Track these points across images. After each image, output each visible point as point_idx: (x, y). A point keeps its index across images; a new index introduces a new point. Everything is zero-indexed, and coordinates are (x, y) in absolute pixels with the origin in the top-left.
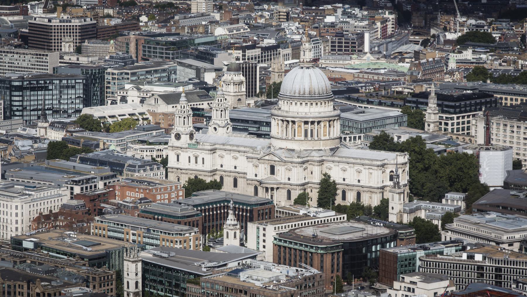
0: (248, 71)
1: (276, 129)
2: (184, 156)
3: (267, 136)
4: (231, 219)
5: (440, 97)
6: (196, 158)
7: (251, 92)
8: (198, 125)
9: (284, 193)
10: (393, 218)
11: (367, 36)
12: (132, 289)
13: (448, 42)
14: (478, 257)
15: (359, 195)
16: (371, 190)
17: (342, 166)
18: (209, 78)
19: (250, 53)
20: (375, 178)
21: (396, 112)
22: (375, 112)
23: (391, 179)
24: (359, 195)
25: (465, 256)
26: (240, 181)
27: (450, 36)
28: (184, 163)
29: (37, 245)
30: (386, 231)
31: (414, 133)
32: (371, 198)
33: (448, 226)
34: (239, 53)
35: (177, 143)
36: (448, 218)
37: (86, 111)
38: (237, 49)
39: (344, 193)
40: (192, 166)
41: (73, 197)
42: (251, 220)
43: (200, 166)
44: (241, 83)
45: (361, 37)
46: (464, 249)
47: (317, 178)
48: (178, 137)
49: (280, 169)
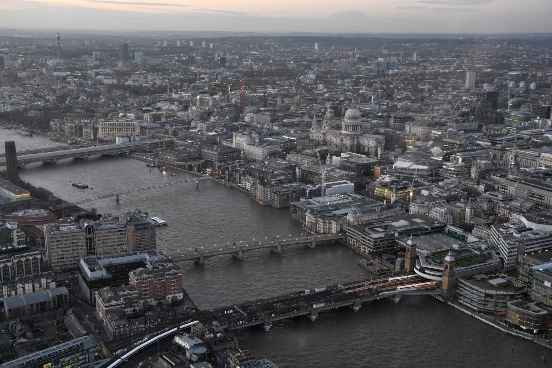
1: (343, 127)
4: (329, 156)
5: (395, 117)
7: (335, 115)
9: (345, 147)
11: (373, 97)
12: (298, 177)
13: (398, 99)
15: (369, 149)
19: (336, 102)
24: (369, 149)
27: (399, 97)
30: (377, 160)
35: (313, 132)
40: (317, 138)
41: (280, 148)
43: (319, 139)
47: (355, 143)
48: (313, 129)
49: (344, 140)
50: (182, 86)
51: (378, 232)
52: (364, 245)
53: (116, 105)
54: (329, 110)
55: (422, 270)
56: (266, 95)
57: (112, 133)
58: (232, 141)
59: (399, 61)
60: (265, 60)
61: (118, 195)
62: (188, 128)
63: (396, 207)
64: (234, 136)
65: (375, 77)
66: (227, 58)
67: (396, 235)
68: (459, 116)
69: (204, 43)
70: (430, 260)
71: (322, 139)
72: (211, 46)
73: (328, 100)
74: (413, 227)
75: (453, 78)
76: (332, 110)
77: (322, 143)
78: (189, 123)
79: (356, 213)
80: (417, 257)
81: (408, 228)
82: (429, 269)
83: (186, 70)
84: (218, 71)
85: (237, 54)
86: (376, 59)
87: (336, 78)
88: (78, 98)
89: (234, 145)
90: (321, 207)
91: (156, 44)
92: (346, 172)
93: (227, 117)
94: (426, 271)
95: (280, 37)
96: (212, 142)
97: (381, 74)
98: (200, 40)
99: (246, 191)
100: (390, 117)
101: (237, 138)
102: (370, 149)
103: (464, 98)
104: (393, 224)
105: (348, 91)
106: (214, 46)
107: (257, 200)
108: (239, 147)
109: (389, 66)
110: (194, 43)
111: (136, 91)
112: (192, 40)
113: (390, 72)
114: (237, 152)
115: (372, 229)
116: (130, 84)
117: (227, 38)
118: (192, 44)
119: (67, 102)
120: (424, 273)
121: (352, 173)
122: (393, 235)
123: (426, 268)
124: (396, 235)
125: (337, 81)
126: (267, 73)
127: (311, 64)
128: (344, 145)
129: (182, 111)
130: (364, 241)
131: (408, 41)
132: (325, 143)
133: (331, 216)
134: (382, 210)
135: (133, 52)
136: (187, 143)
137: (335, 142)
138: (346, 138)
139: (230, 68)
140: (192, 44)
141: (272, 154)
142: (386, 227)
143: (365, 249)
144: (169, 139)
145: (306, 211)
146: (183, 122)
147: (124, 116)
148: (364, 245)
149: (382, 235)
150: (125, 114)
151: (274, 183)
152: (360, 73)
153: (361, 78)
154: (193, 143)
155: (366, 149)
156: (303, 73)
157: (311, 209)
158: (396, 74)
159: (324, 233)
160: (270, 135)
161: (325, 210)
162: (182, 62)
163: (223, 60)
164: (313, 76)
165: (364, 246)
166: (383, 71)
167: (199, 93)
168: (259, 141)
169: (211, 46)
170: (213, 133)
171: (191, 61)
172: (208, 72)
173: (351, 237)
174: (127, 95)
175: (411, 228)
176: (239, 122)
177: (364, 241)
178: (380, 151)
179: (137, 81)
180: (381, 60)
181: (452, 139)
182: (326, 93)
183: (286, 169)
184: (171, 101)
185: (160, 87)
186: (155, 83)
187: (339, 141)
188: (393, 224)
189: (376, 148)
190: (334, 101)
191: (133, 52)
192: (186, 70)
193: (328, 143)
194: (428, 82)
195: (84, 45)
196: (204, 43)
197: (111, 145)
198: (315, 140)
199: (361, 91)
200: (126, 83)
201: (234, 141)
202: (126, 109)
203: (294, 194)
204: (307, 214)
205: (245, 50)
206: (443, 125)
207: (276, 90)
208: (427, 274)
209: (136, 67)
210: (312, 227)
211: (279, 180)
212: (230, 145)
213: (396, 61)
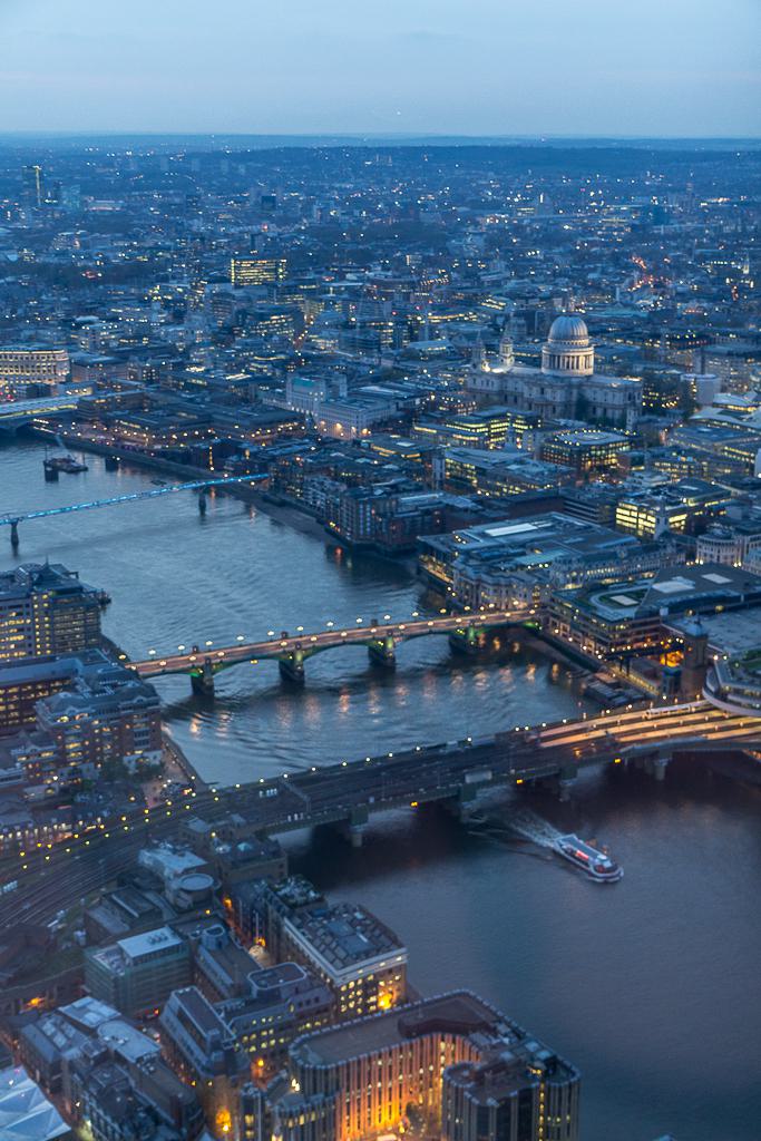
0: (528, 316)
1: (544, 360)
2: (479, 381)
6: (488, 381)
9: (550, 408)
15: (605, 410)
16: (614, 407)
17: (594, 389)
18: (500, 321)
20: (619, 399)
23: (630, 398)
24: (605, 410)
26: (520, 400)
32: (613, 414)
34: (524, 301)
38: (522, 298)
39: (594, 409)
40: (484, 388)
41: (398, 409)
43: (490, 388)
44: (523, 325)
49: (548, 391)
51: (621, 606)
54: (513, 321)
58: (282, 397)
61: (14, 524)
62: (181, 366)
63: (665, 547)
64: (289, 385)
65: (628, 241)
67: (664, 612)
71: (496, 388)
72: (242, 170)
73: (512, 296)
74: (704, 594)
76: (522, 321)
78: (186, 354)
79: (570, 562)
80: (711, 663)
81: (691, 597)
82: (737, 692)
83: (179, 228)
84: (255, 228)
85: (299, 188)
90: (489, 548)
92: (552, 466)
94: (730, 697)
95: (404, 149)
97: (639, 232)
98: (218, 156)
99: (315, 511)
101: (297, 388)
102: (609, 414)
105: (560, 275)
109: (661, 216)
111: (63, 277)
113: (662, 230)
114: (295, 419)
115: (607, 600)
116: (47, 260)
122: (657, 613)
124: (664, 612)
126: (373, 235)
127: (477, 212)
128: (548, 403)
129: (167, 324)
134: (632, 554)
137: (526, 395)
138: (551, 386)
139: (281, 222)
140: (195, 165)
141: (379, 424)
142: (638, 595)
146: (171, 351)
149: (631, 613)
150: (32, 332)
151: (379, 492)
153: (592, 244)
154: (191, 400)
155: (599, 412)
156: (456, 232)
157: (467, 554)
158: (674, 237)
159: (496, 609)
160: (375, 380)
161: (500, 556)
164: (480, 242)
166: (644, 227)
168: (349, 395)
169: (242, 170)
170: (240, 376)
172: (233, 230)
175: (698, 595)
178: (631, 417)
179: (63, 253)
182: (509, 279)
184: (145, 303)
187: (535, 392)
188: (656, 586)
190: (527, 299)
191: (57, 186)
192: (179, 228)
193: (511, 399)
194: (750, 252)
198: (481, 392)
199: (591, 276)
203: (427, 518)
208: (732, 702)
209: (64, 223)
211: (392, 486)
212: (281, 405)
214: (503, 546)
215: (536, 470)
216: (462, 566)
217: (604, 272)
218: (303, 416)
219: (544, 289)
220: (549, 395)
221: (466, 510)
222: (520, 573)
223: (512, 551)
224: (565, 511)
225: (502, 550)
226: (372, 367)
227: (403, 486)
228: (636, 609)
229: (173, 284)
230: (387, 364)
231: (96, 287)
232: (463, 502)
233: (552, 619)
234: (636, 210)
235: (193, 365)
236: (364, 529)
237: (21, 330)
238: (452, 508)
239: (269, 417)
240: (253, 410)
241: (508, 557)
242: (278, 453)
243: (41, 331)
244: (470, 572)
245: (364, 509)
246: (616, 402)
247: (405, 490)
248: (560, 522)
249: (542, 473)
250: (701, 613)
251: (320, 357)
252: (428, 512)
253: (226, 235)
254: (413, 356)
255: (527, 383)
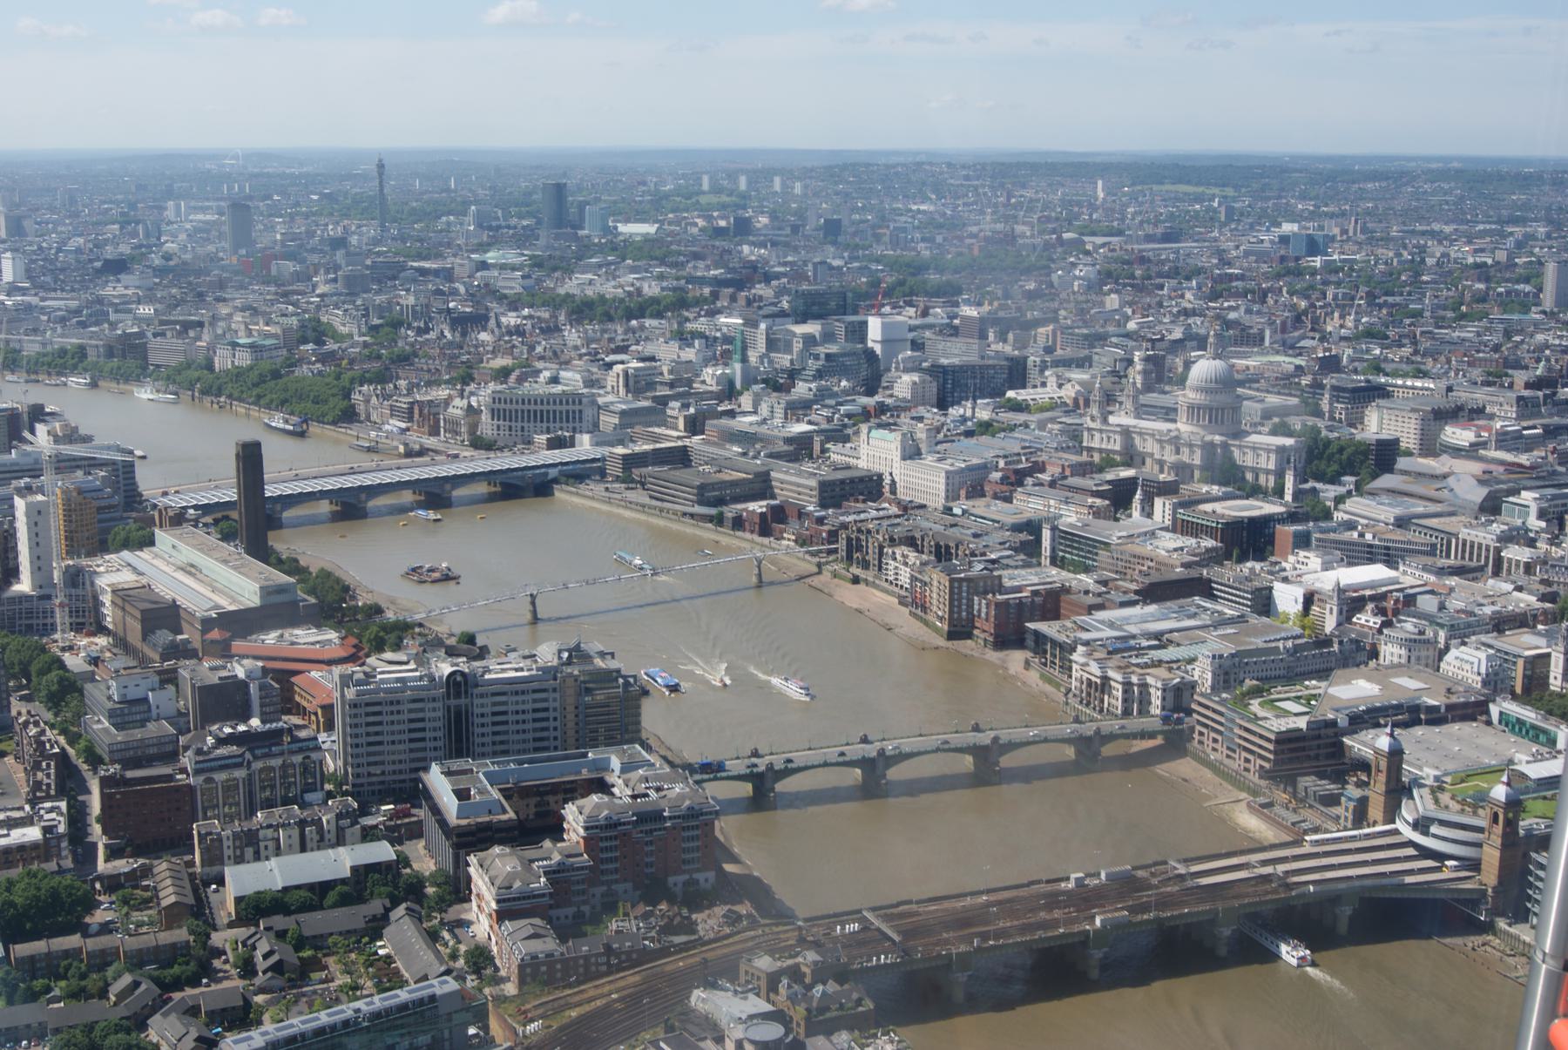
2: (1097, 435)
3: (1175, 421)
8: (1110, 409)
10: (1288, 497)
11: (1267, 333)
14: (1369, 536)
16: (1268, 472)
21: (1295, 401)
22: (1273, 400)
25: (1355, 535)
28: (1096, 444)
29: (964, 512)
30: (1282, 509)
31: (1311, 420)
33: (1341, 506)
35: (1092, 425)
36: (1339, 500)
37: (1010, 394)
42: (1159, 495)
45: (1262, 332)
46: (1355, 528)
48: (1093, 419)
50: (715, 296)
51: (1286, 713)
52: (1246, 749)
53: (532, 348)
55: (1421, 825)
56: (956, 322)
57: (519, 424)
59: (1344, 232)
60: (953, 225)
66: (845, 222)
68: (1528, 386)
69: (777, 180)
70: (1445, 798)
72: (798, 188)
75: (1507, 281)
77: (1118, 458)
82: (1443, 823)
86: (1279, 225)
87: (1160, 275)
88: (427, 330)
89: (862, 464)
91: (644, 183)
92: (1192, 542)
93: (844, 383)
94: (1434, 829)
96: (800, 449)
97: (1289, 269)
98: (768, 174)
100: (1322, 387)
102: (1262, 479)
103: (1540, 337)
104: (1331, 691)
106: (806, 187)
107: (930, 618)
108: (877, 468)
110: (749, 183)
112: (742, 171)
113: (1317, 261)
117: (844, 167)
118: (743, 184)
119: (400, 344)
120: (1426, 833)
121: (1209, 543)
123: (1432, 820)
125: (1161, 287)
130: (1246, 740)
131: (1374, 176)
132: (1131, 457)
133: (1146, 666)
135: (581, 207)
136: (727, 454)
143: (1247, 761)
144: (680, 443)
145: (1074, 649)
147: (555, 380)
148: (1246, 749)
149: (1302, 723)
152: (1229, 264)
162: (719, 232)
163: (832, 229)
165: (1244, 754)
167: (766, 317)
169: (798, 188)
171: (743, 228)
173: (1206, 726)
174: (562, 318)
176: (878, 398)
177: (1246, 740)
180: (1288, 228)
181: (1508, 451)
183: (1017, 528)
185: (654, 301)
186: (639, 291)
189: (1280, 475)
191: (581, 207)
195: (448, 190)
196: (777, 180)
197: (516, 459)
200: (561, 291)
201: (864, 450)
202: (557, 357)
204: (1075, 657)
205: (895, 199)
206: (1479, 412)
207: (986, 308)
208: (1435, 836)
209: (586, 249)
210: (1089, 694)
211: (993, 562)
212: (853, 461)
213: (1336, 231)
214: (1134, 637)
215: (1172, 545)
216: (1082, 660)
217: (1249, 311)
218: (880, 476)
219: (1178, 334)
220: (1185, 457)
221: (1087, 592)
222: (1162, 672)
223: (1145, 643)
224: (1209, 594)
225: (1132, 642)
226: (964, 419)
227: (1005, 561)
228: (1306, 718)
229: (723, 320)
230: (984, 415)
231: (629, 320)
232: (1087, 580)
233: (1198, 728)
234: (1284, 240)
235: (744, 413)
236: (959, 613)
237: (540, 371)
238: (1066, 590)
239: (840, 475)
240: (818, 468)
241: (1140, 651)
242: (851, 518)
243: (563, 374)
244: (1094, 668)
245: (960, 588)
246: (1272, 466)
247: (1008, 567)
248: (1206, 609)
249: (1182, 549)
250: (1395, 725)
251: (897, 408)
252: (1035, 593)
253: (785, 264)
254: (1018, 407)
255: (1160, 441)
